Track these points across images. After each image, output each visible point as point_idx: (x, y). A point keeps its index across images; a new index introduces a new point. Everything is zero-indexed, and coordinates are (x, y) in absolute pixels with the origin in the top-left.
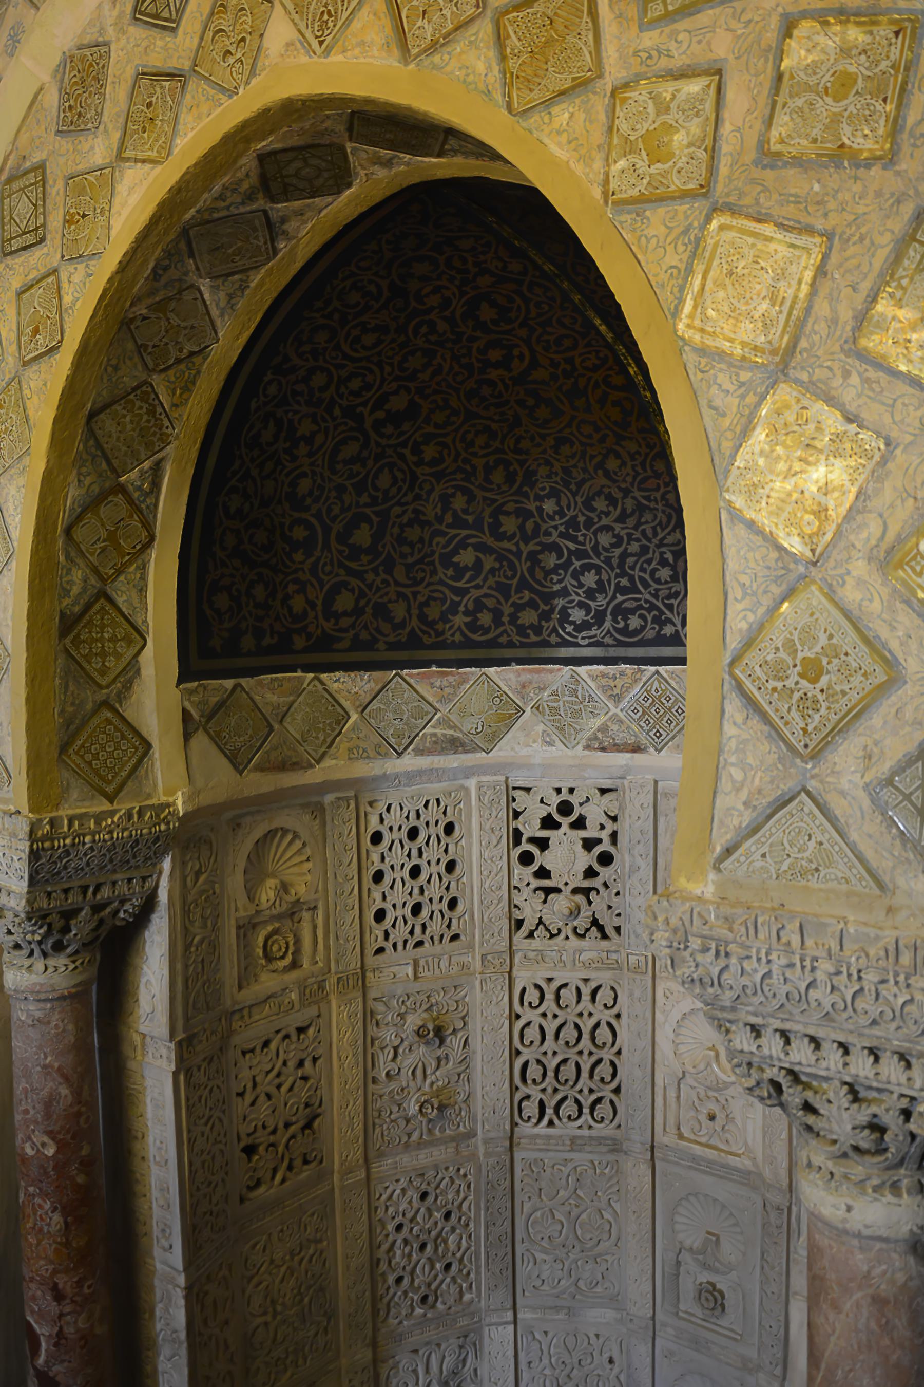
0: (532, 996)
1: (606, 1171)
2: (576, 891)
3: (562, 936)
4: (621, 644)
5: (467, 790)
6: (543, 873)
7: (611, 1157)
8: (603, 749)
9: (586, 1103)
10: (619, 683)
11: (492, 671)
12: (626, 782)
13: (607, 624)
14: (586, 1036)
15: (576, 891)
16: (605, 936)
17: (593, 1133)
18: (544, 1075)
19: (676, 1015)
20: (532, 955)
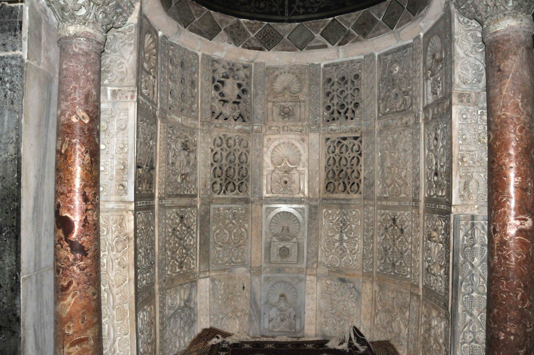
0: (218, 141)
1: (243, 212)
2: (234, 102)
3: (228, 120)
4: (256, 12)
5: (198, 56)
6: (222, 94)
7: (245, 206)
8: (249, 48)
9: (237, 184)
10: (255, 26)
11: (212, 12)
12: (253, 64)
13: (253, 4)
14: (237, 158)
15: (234, 102)
16: (244, 121)
17: (240, 197)
18: (222, 173)
19: (272, 147)
20: (218, 125)
